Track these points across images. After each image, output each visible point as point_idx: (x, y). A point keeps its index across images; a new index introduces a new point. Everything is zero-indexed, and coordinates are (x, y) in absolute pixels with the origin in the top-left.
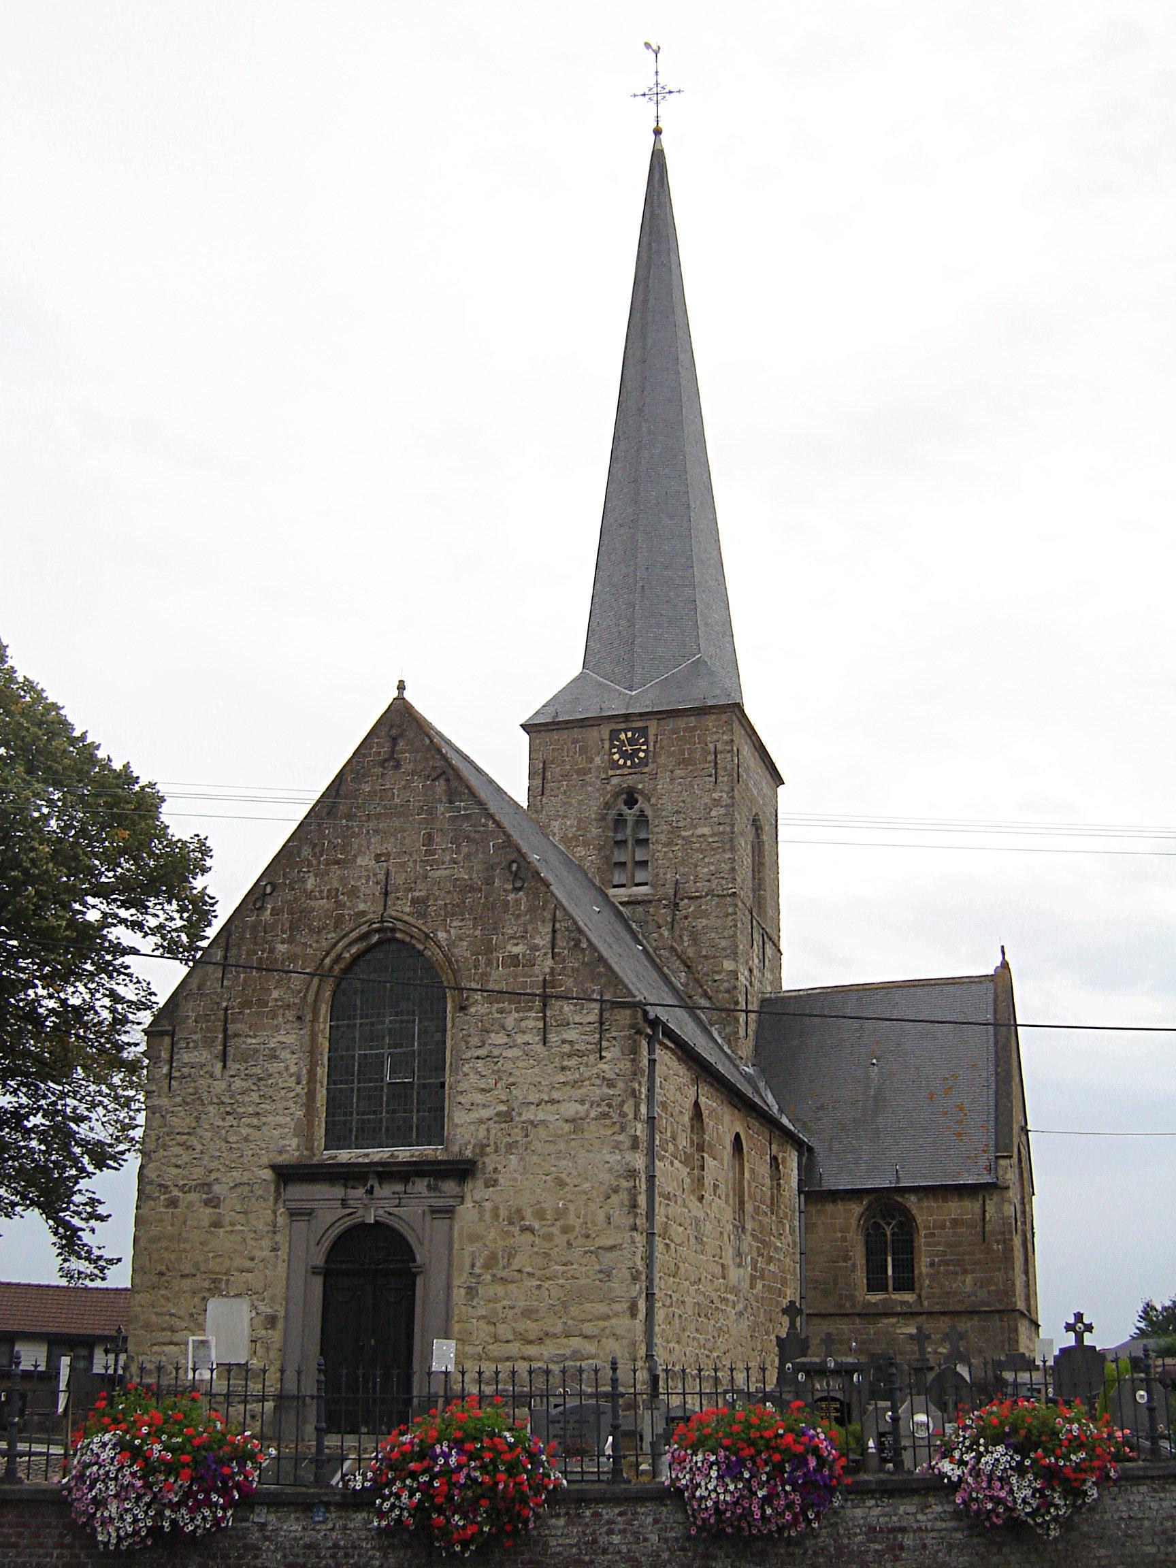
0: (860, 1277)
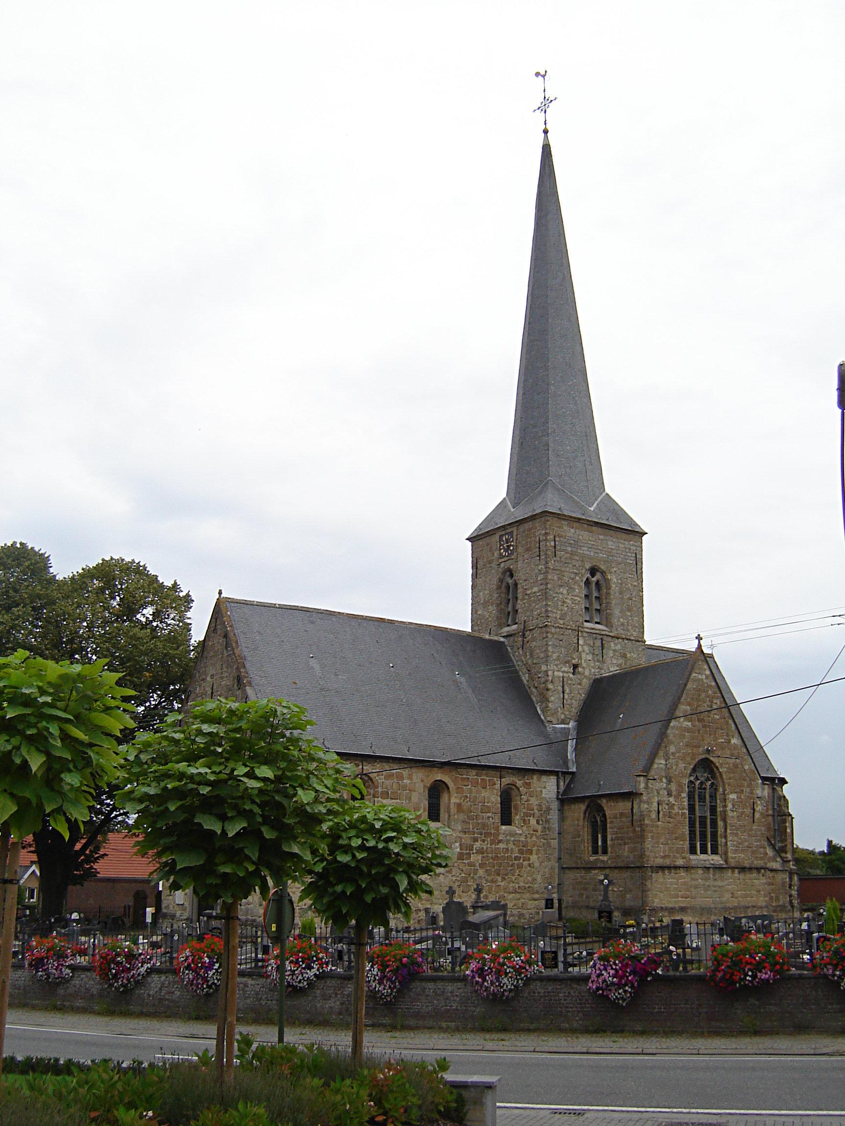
0: (587, 846)
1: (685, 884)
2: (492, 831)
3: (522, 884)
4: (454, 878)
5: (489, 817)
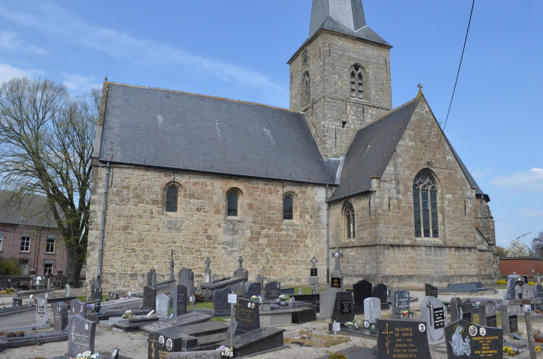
0: (344, 233)
1: (412, 258)
2: (276, 223)
3: (299, 258)
4: (246, 254)
5: (274, 213)
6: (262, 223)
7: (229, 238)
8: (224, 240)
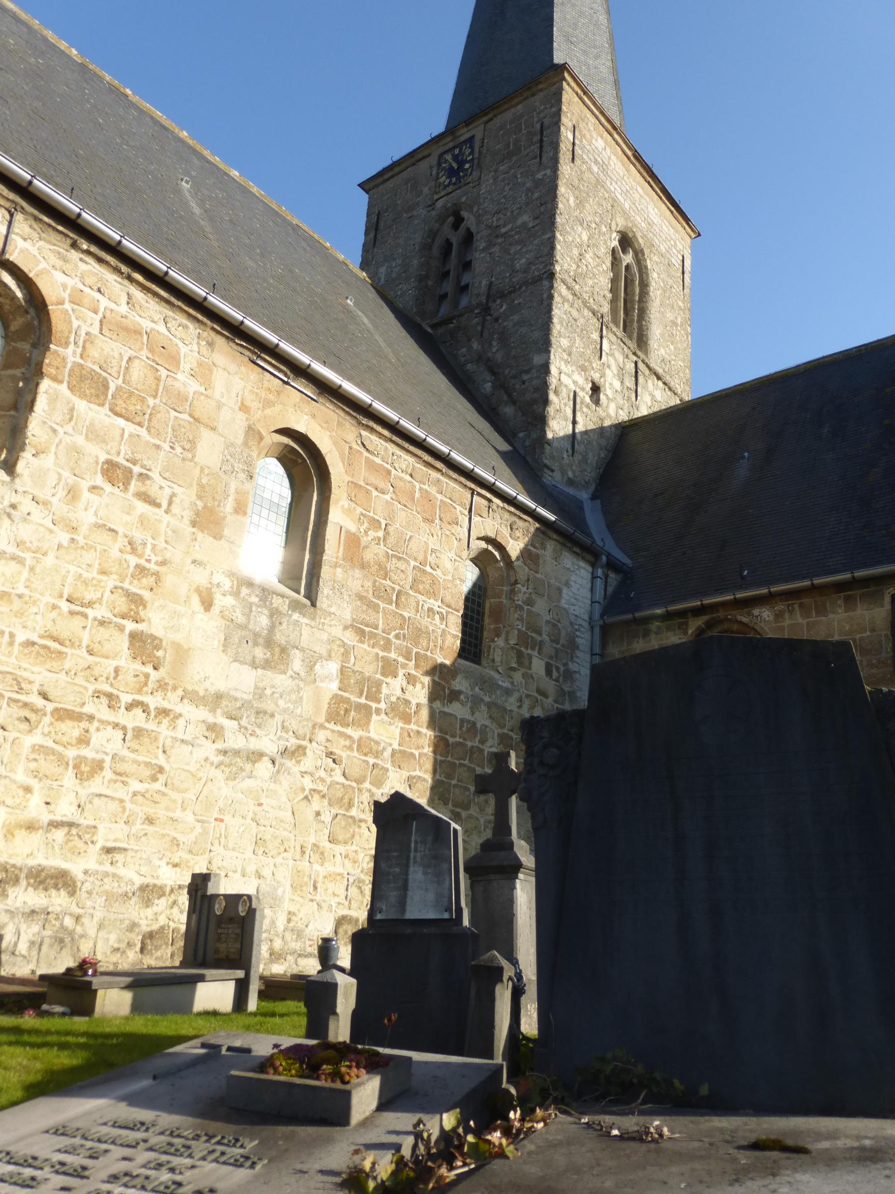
6: (387, 646)
7: (241, 680)
8: (221, 685)
